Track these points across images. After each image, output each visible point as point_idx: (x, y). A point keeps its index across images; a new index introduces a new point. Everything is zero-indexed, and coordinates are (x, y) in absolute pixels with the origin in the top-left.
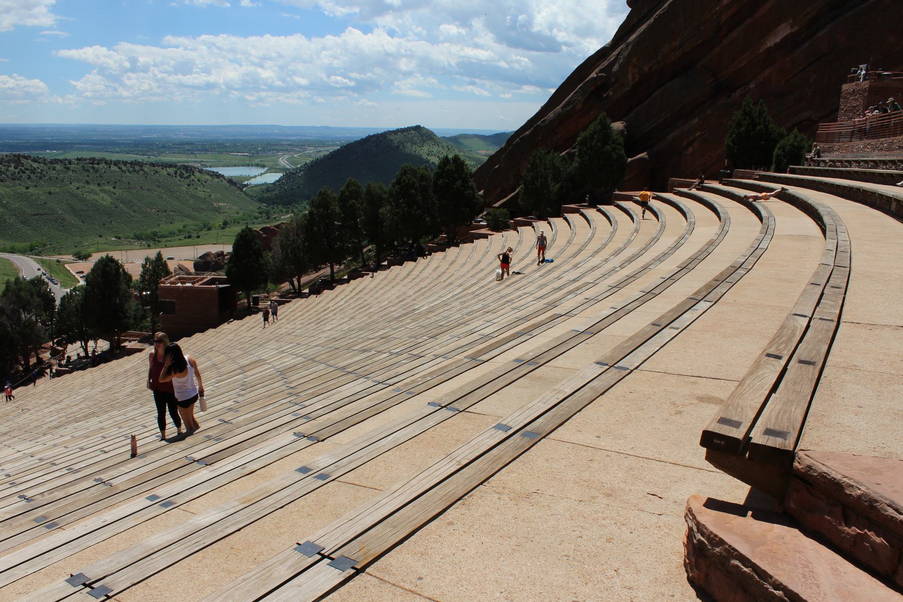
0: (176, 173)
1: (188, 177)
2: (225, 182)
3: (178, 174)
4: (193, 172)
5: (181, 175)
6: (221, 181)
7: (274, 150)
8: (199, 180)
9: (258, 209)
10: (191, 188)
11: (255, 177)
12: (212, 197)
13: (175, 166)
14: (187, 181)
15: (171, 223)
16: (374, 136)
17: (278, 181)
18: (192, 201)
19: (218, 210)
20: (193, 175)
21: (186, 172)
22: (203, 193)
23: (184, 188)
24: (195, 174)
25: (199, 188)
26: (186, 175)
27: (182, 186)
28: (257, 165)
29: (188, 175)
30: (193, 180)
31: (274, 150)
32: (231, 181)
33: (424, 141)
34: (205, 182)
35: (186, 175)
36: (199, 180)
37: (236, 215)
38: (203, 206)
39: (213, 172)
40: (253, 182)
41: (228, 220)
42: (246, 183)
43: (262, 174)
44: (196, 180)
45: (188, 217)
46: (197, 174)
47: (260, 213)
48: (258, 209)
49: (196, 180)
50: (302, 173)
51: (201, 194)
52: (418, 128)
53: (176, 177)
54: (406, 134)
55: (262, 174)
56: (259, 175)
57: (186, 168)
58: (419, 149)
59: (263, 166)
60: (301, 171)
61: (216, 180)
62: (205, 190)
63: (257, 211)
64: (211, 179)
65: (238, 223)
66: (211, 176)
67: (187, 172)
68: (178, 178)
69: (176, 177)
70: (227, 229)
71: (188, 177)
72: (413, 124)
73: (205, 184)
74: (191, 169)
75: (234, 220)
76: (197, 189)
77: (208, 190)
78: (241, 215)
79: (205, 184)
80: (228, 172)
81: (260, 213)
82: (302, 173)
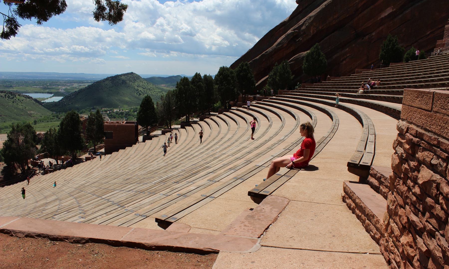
0: (5, 96)
1: (12, 98)
2: (33, 101)
3: (7, 96)
4: (15, 96)
5: (9, 97)
6: (31, 100)
7: (56, 85)
8: (19, 100)
9: (52, 114)
10: (15, 104)
11: (47, 98)
12: (27, 108)
13: (5, 92)
14: (12, 100)
15: (5, 122)
16: (110, 77)
17: (61, 100)
18: (15, 111)
19: (30, 115)
20: (15, 97)
21: (11, 95)
22: (22, 106)
23: (11, 104)
24: (16, 97)
25: (19, 104)
26: (11, 97)
27: (9, 103)
28: (48, 93)
29: (12, 97)
30: (15, 100)
31: (56, 85)
32: (36, 100)
33: (135, 80)
34: (22, 101)
35: (11, 97)
36: (19, 100)
37: (40, 118)
38: (22, 113)
39: (26, 96)
40: (47, 101)
41: (37, 120)
42: (43, 101)
43: (51, 97)
44: (17, 99)
45: (14, 119)
46: (17, 97)
47: (53, 116)
48: (52, 114)
49: (17, 99)
50: (74, 96)
51: (20, 107)
52: (132, 73)
53: (6, 98)
54: (126, 76)
55: (51, 97)
56: (49, 98)
57: (11, 93)
58: (133, 84)
59: (51, 93)
60: (73, 95)
61: (28, 100)
62: (23, 105)
63: (52, 115)
64: (25, 99)
65: (43, 121)
66: (25, 97)
67: (12, 95)
68: (7, 98)
69: (6, 98)
70: (37, 125)
71: (12, 98)
72: (130, 71)
73: (22, 102)
74: (14, 94)
75: (40, 120)
76: (18, 104)
77: (24, 105)
78: (43, 117)
79: (22, 102)
80: (34, 96)
81: (53, 116)
82: (74, 96)
